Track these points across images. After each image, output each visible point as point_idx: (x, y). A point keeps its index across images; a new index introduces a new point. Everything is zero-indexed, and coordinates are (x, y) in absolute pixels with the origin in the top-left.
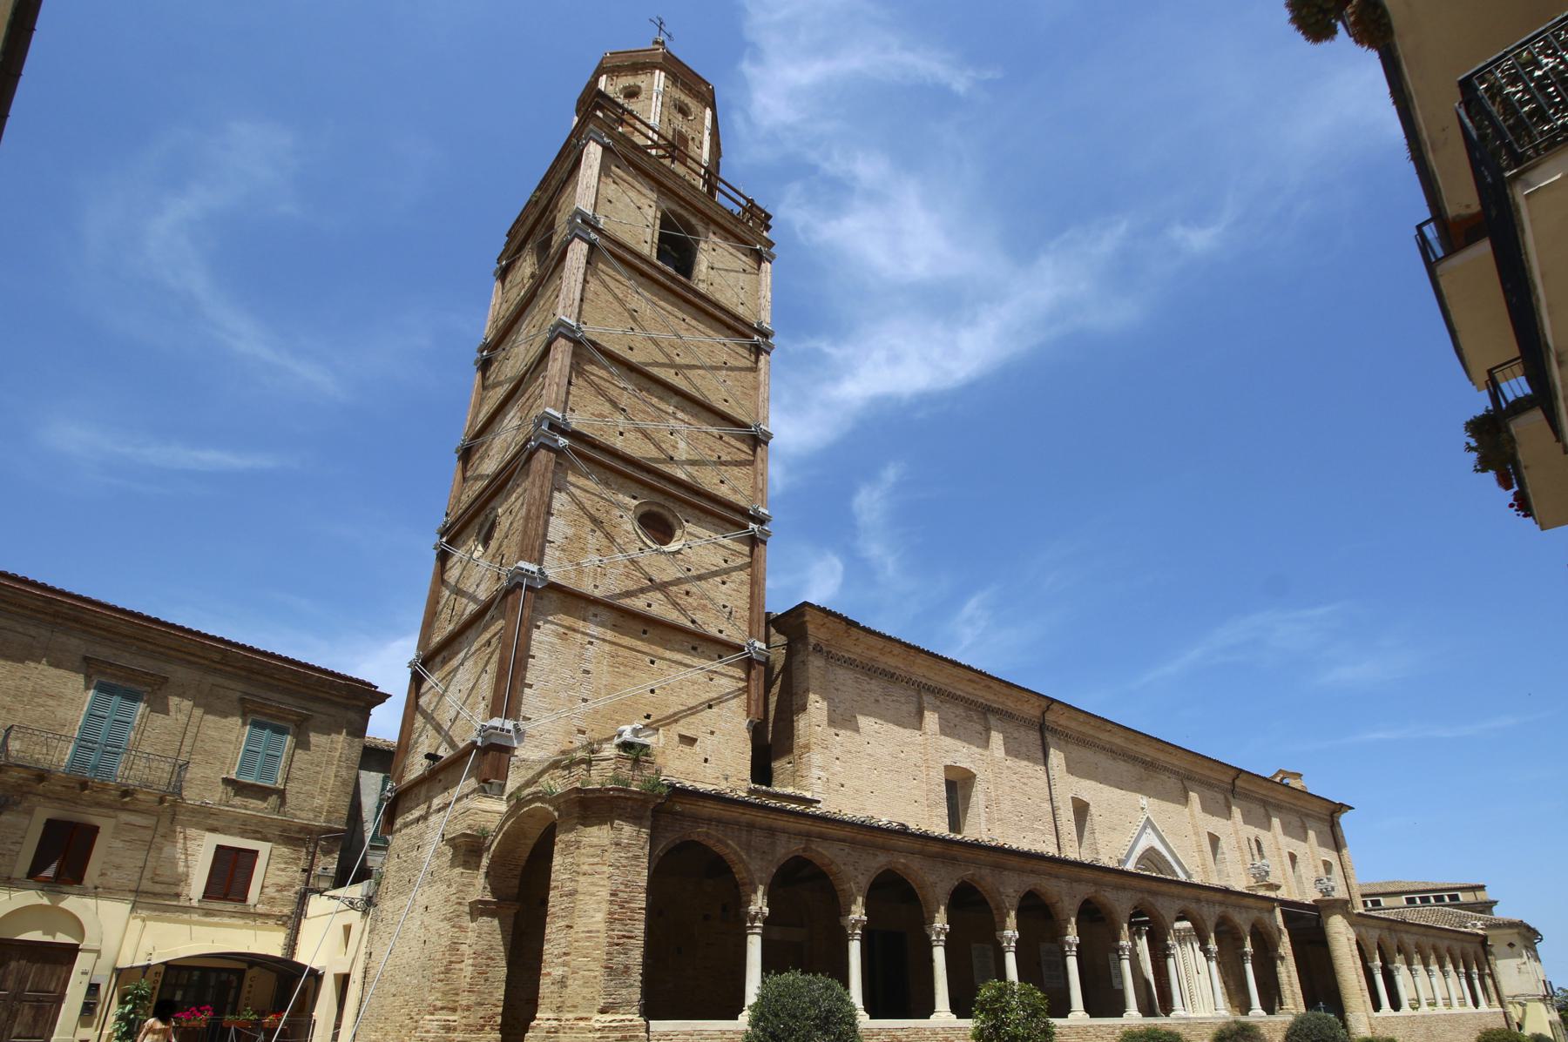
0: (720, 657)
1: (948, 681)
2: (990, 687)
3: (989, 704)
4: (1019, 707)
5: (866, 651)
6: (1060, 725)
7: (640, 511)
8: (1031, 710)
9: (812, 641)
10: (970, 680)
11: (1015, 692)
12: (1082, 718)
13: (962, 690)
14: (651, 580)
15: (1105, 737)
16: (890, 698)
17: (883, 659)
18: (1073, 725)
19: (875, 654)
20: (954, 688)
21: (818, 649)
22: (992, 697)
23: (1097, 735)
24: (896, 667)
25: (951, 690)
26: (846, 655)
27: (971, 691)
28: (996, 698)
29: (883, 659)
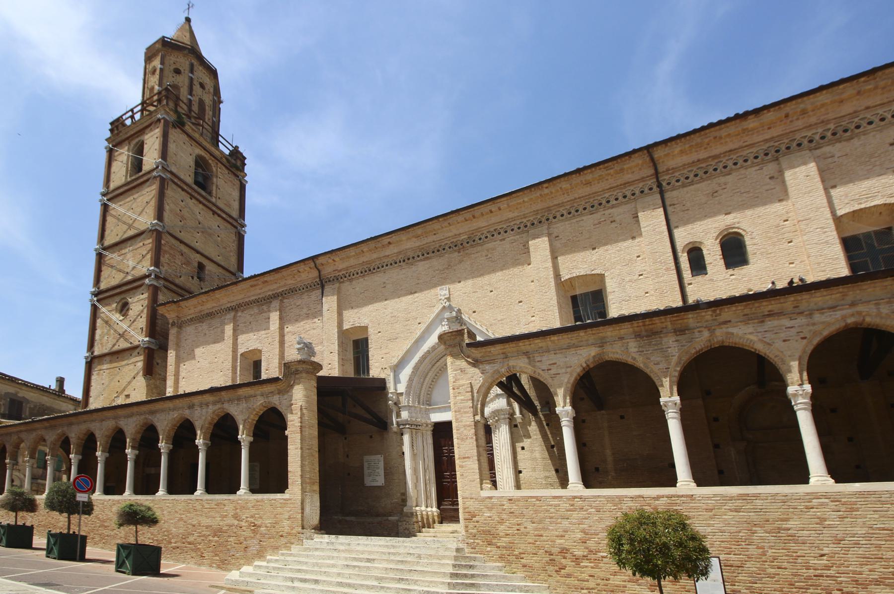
0: (131, 355)
1: (242, 296)
2: (266, 281)
3: (274, 292)
4: (299, 279)
5: (195, 309)
6: (340, 271)
7: (119, 308)
8: (308, 275)
9: (171, 321)
10: (252, 286)
11: (284, 273)
12: (352, 252)
13: (253, 296)
14: (120, 335)
15: (391, 250)
16: (212, 328)
17: (204, 308)
18: (352, 262)
19: (199, 308)
20: (249, 297)
21: (173, 324)
22: (275, 286)
23: (382, 255)
24: (213, 307)
25: (247, 300)
26: (189, 318)
27: (259, 291)
28: (278, 285)
29: (204, 308)
